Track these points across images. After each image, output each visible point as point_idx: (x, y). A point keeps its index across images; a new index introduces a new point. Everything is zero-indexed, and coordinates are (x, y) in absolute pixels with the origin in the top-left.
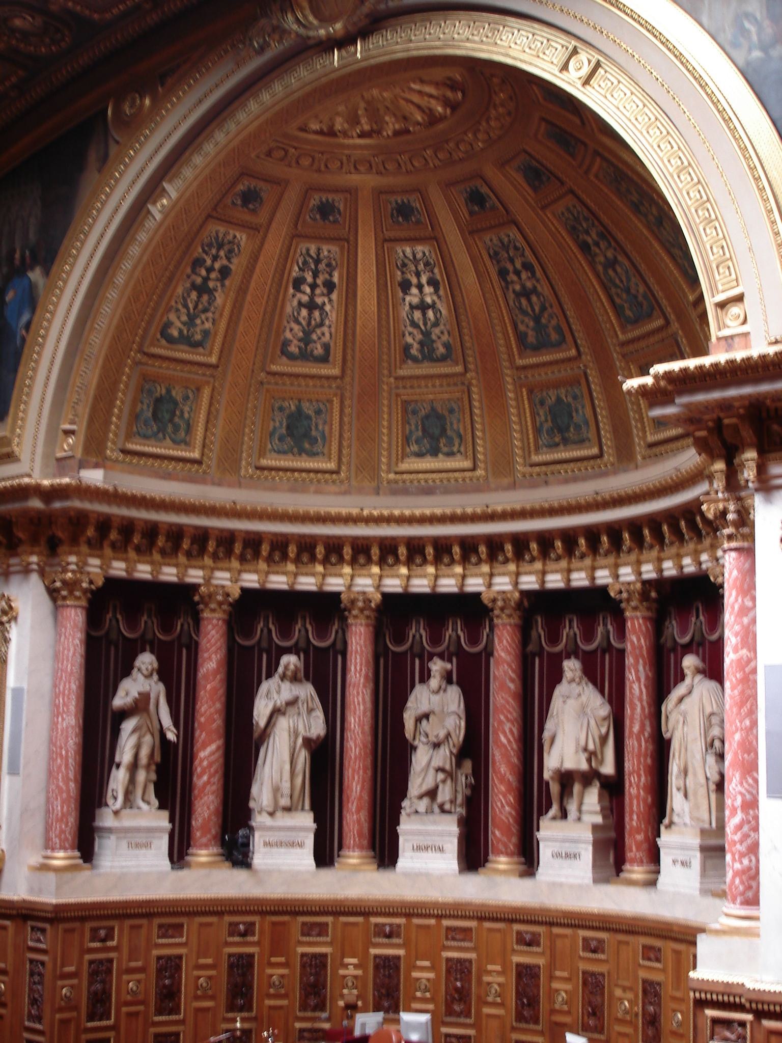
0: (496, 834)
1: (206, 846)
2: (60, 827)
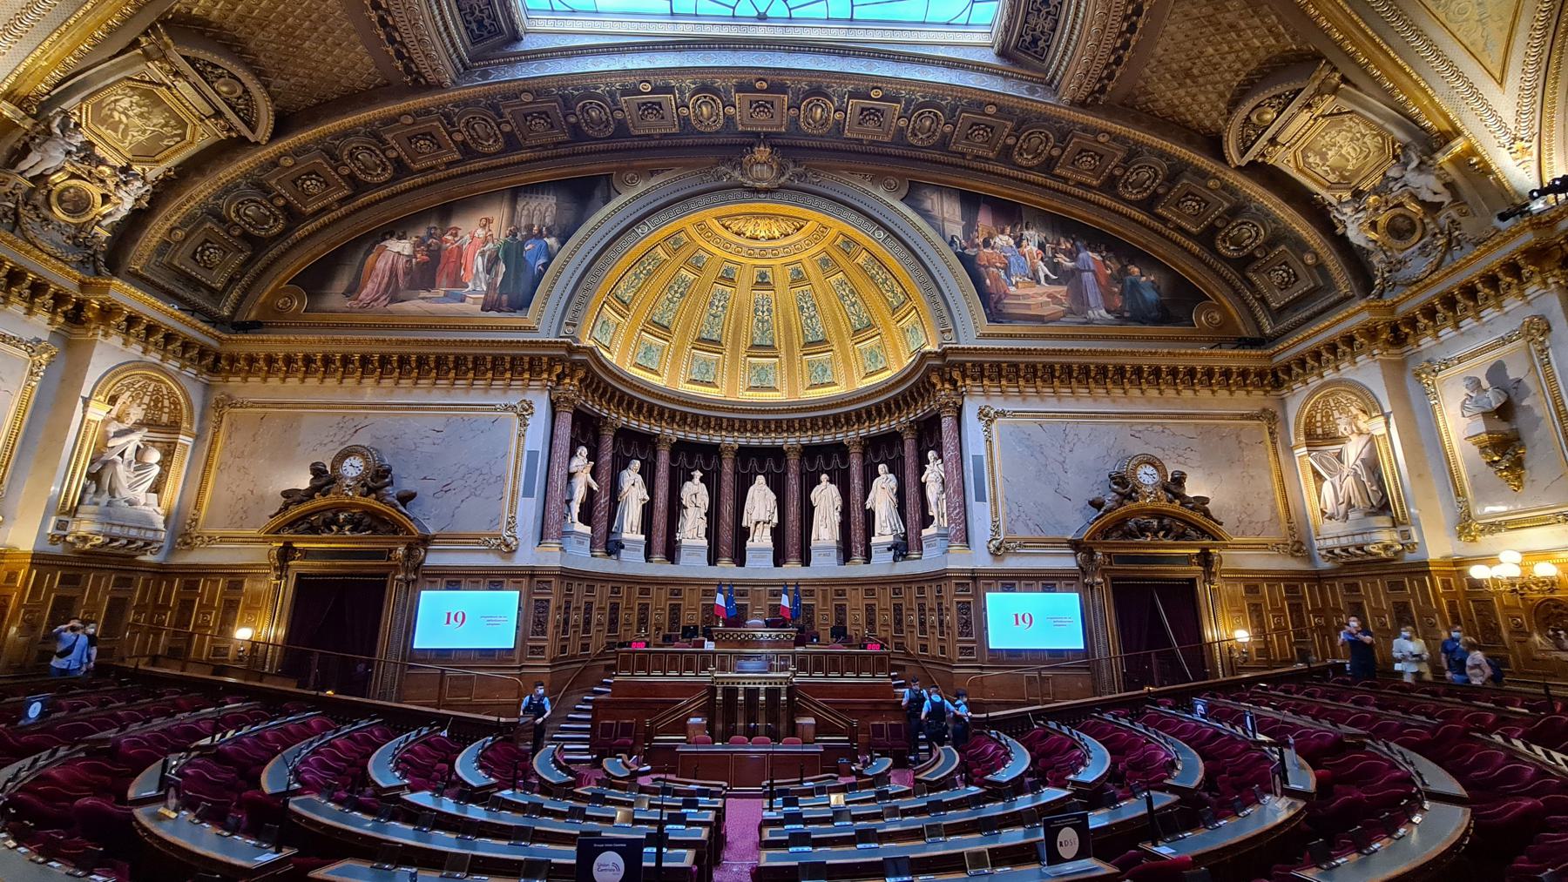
0: (724, 549)
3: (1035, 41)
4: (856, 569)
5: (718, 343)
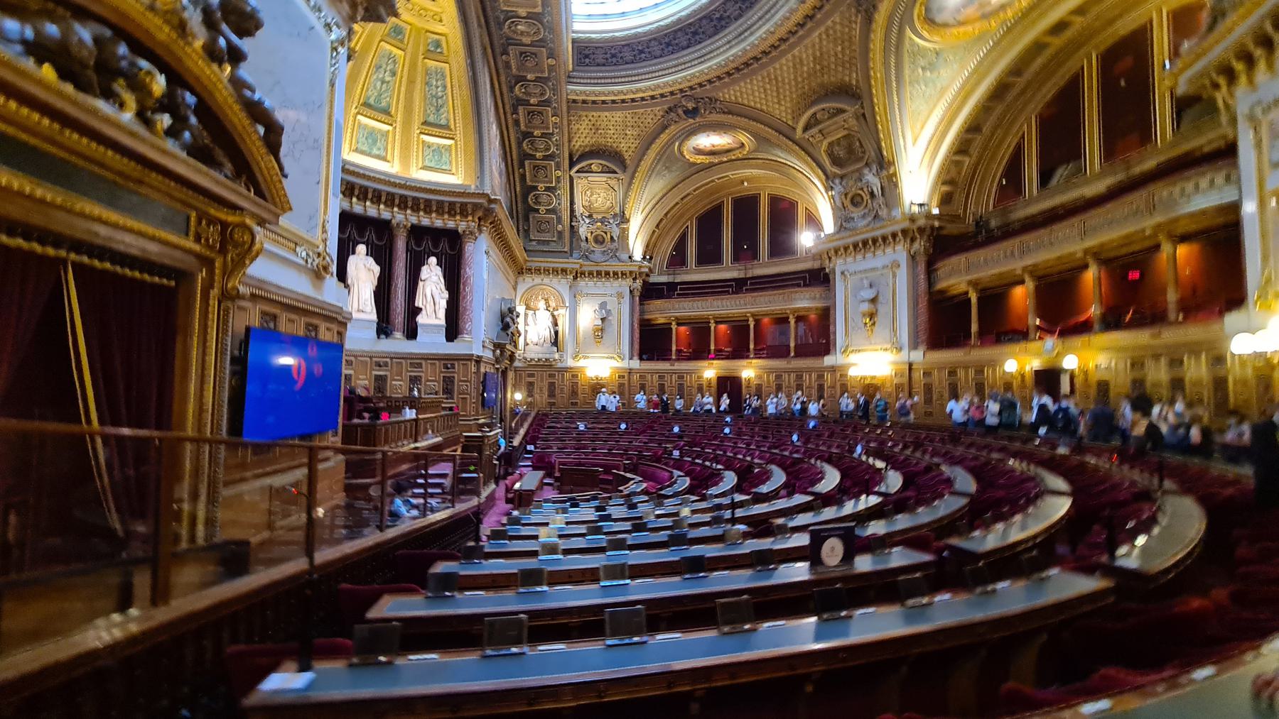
3: (587, 56)
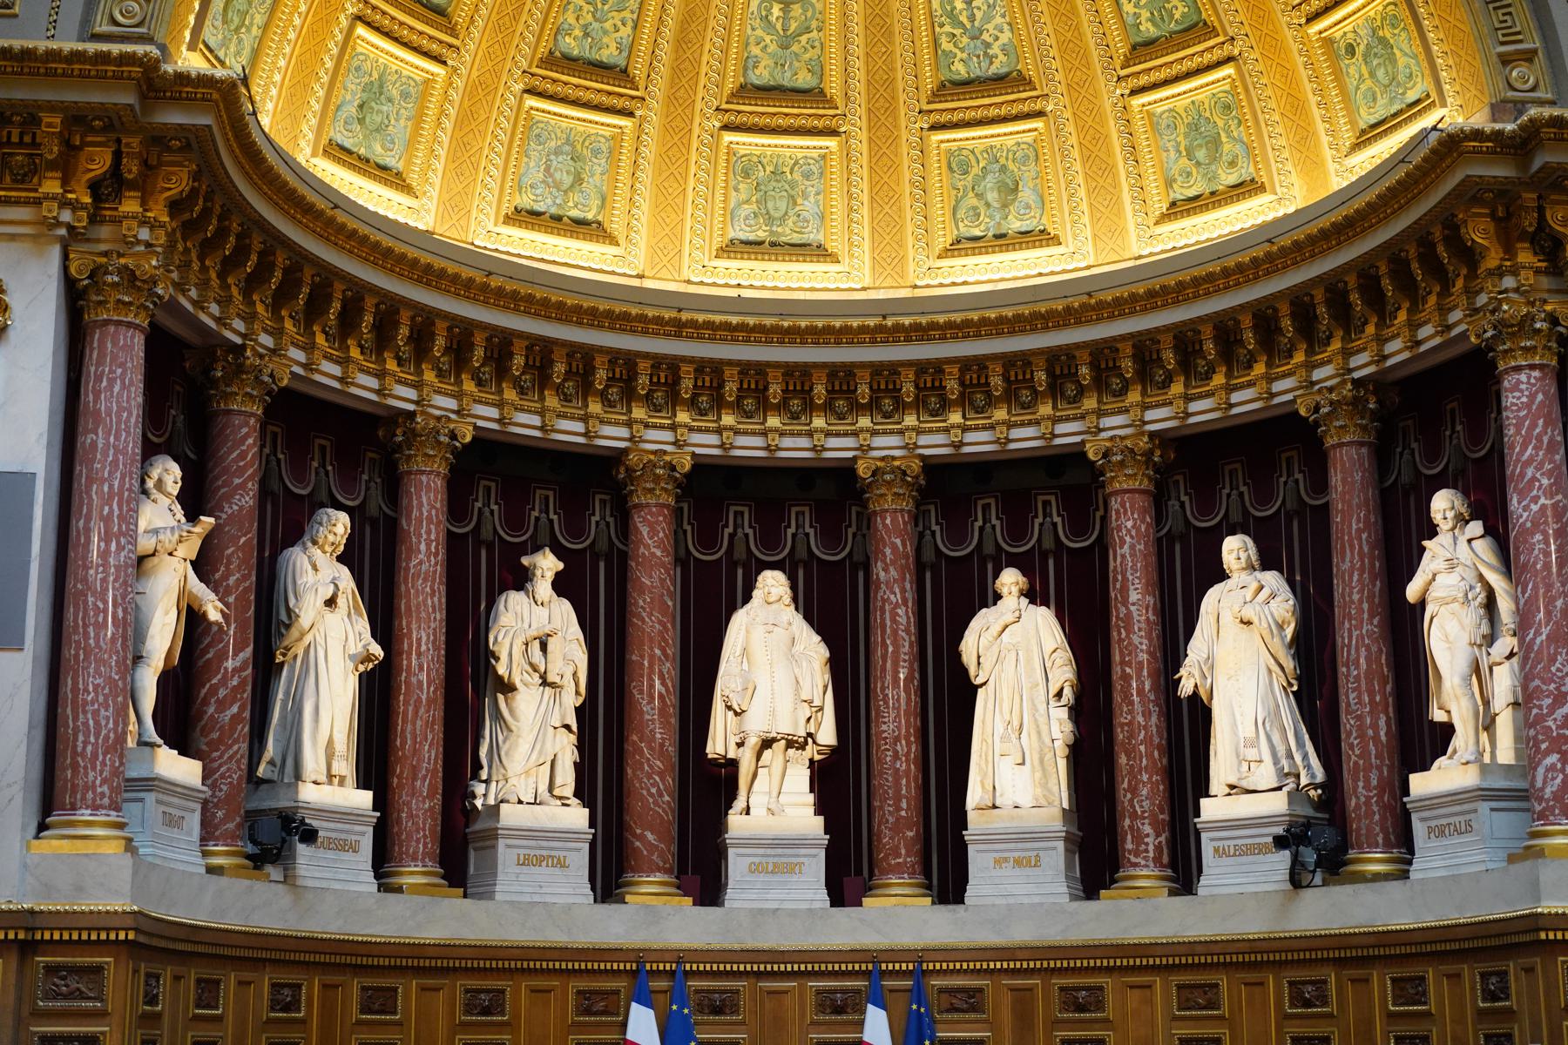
1: (230, 838)
2: (112, 765)
4: (1141, 913)
5: (620, 74)
